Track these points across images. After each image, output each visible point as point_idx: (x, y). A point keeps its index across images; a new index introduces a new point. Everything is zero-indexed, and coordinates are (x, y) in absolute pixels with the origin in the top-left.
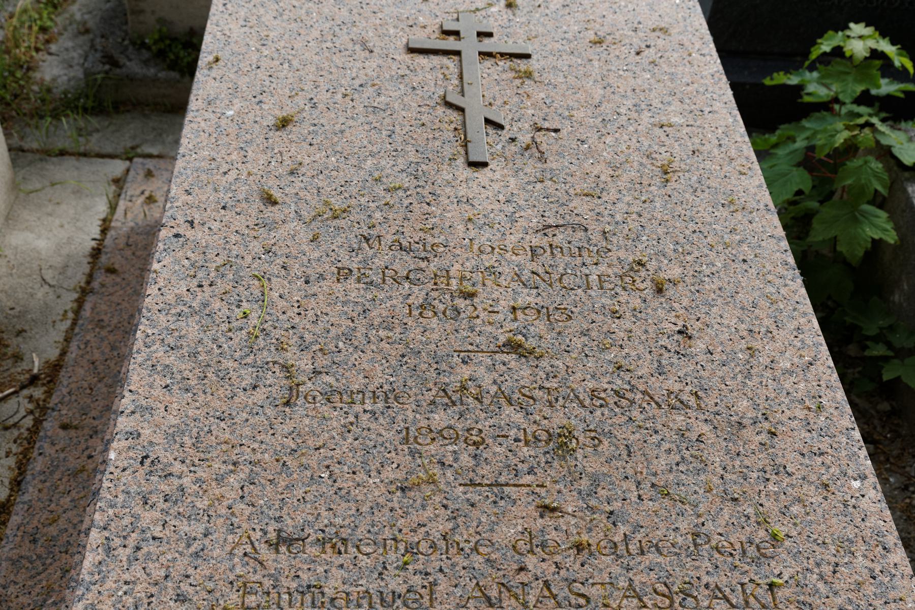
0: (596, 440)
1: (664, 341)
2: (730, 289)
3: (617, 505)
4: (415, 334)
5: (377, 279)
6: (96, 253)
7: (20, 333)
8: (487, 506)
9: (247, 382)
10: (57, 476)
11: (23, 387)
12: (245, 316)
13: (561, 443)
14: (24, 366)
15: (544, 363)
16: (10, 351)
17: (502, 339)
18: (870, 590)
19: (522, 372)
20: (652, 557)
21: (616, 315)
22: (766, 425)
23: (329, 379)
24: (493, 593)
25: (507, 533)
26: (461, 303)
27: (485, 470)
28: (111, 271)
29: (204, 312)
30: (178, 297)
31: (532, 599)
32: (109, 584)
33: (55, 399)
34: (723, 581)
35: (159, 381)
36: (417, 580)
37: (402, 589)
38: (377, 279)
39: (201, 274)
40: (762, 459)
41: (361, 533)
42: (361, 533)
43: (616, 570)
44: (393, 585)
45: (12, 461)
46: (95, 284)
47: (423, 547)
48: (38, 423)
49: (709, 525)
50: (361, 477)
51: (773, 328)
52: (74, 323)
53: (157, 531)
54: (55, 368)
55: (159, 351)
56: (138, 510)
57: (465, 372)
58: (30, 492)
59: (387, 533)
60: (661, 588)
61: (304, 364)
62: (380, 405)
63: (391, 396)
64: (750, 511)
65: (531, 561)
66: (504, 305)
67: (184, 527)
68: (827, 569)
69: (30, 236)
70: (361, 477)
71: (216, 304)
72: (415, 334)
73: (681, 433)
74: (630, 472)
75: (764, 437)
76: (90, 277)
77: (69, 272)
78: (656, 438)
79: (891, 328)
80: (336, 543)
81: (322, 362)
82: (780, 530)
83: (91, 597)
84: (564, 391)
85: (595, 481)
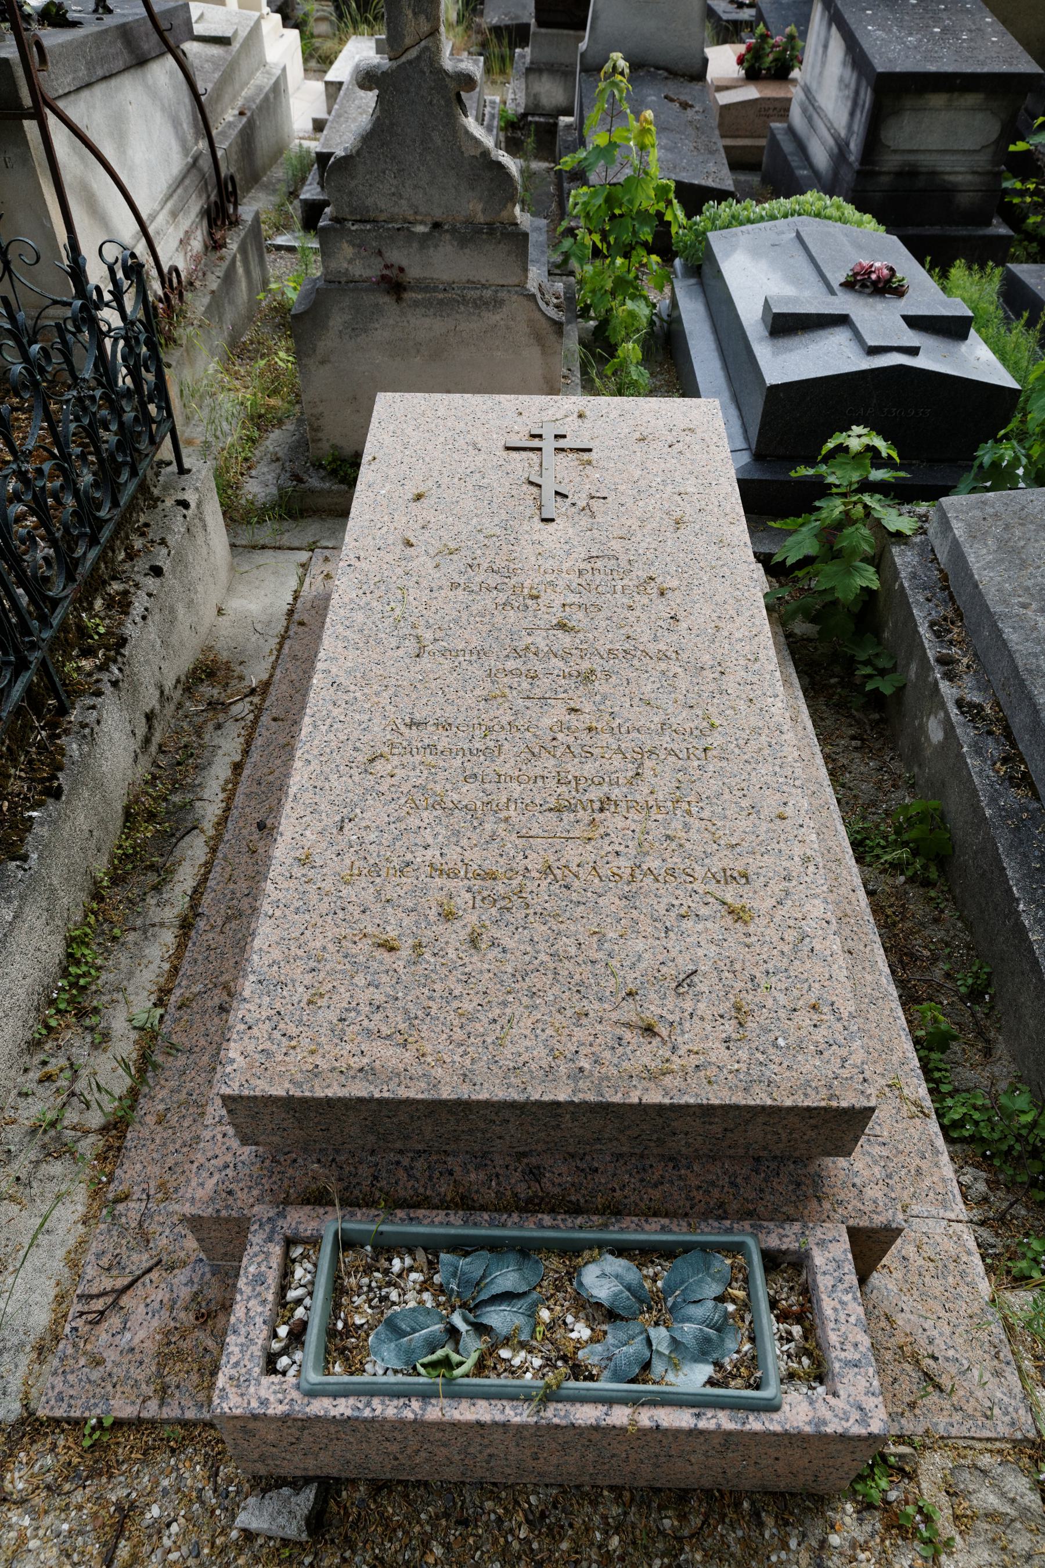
0: (608, 676)
1: (661, 623)
2: (709, 594)
3: (616, 709)
4: (498, 619)
5: (476, 589)
6: (291, 613)
7: (241, 663)
8: (537, 709)
9: (394, 645)
10: (271, 748)
11: (246, 696)
12: (392, 609)
13: (587, 677)
14: (246, 683)
15: (580, 635)
16: (236, 674)
17: (555, 622)
18: (766, 752)
19: (565, 640)
20: (634, 734)
21: (631, 608)
22: (719, 669)
23: (444, 644)
24: (536, 750)
25: (547, 722)
26: (529, 602)
27: (537, 691)
28: (301, 624)
29: (368, 608)
30: (351, 600)
31: (558, 754)
32: (316, 742)
33: (267, 704)
34: (675, 747)
35: (340, 644)
36: (492, 744)
37: (483, 748)
38: (476, 589)
39: (365, 587)
40: (713, 686)
41: (458, 721)
42: (458, 721)
43: (611, 740)
44: (477, 745)
45: (242, 740)
46: (291, 633)
47: (496, 728)
48: (257, 718)
49: (672, 720)
50: (461, 693)
51: (735, 615)
52: (278, 657)
53: (342, 718)
54: (267, 685)
55: (340, 629)
56: (331, 707)
57: (530, 640)
58: (255, 756)
59: (475, 721)
60: (637, 749)
61: (428, 635)
62: (475, 657)
63: (481, 653)
64: (700, 713)
65: (560, 736)
66: (557, 604)
67: (357, 717)
68: (741, 742)
69: (244, 602)
70: (461, 693)
71: (375, 604)
72: (498, 619)
73: (663, 673)
74: (627, 692)
75: (717, 675)
76: (287, 629)
77: (273, 625)
78: (646, 675)
79: (877, 655)
80: (447, 726)
81: (439, 634)
82: (717, 723)
83: (307, 747)
84: (591, 650)
85: (605, 698)
